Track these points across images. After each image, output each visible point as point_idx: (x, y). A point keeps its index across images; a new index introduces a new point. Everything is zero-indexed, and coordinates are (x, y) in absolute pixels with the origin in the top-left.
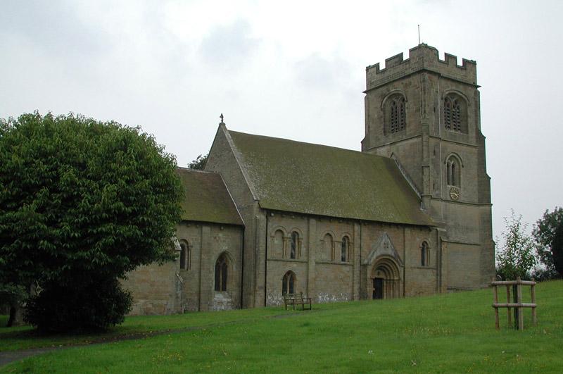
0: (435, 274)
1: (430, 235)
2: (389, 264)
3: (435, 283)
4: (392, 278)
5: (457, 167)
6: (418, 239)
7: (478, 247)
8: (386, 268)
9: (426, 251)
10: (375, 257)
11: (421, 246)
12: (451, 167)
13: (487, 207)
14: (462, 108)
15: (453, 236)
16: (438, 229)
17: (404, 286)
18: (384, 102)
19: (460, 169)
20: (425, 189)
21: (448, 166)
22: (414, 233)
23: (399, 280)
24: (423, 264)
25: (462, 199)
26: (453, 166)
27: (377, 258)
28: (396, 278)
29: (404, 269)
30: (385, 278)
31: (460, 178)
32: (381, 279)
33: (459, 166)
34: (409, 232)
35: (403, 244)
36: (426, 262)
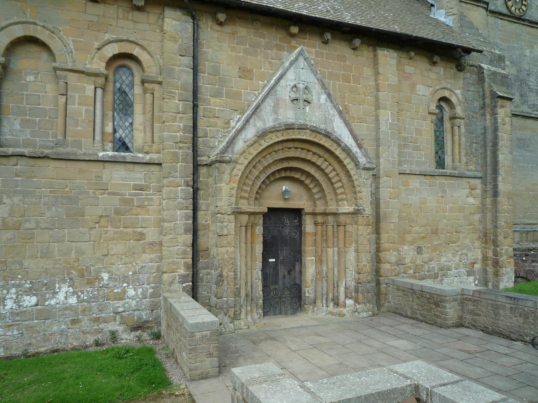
0: (478, 191)
2: (314, 159)
3: (477, 217)
4: (332, 208)
6: (421, 89)
8: (308, 175)
9: (447, 125)
10: (250, 133)
11: (433, 108)
17: (377, 231)
22: (409, 69)
23: (356, 213)
24: (440, 163)
27: (262, 135)
28: (346, 208)
29: (376, 177)
30: (308, 209)
32: (298, 213)
34: (394, 62)
35: (370, 99)
36: (448, 160)
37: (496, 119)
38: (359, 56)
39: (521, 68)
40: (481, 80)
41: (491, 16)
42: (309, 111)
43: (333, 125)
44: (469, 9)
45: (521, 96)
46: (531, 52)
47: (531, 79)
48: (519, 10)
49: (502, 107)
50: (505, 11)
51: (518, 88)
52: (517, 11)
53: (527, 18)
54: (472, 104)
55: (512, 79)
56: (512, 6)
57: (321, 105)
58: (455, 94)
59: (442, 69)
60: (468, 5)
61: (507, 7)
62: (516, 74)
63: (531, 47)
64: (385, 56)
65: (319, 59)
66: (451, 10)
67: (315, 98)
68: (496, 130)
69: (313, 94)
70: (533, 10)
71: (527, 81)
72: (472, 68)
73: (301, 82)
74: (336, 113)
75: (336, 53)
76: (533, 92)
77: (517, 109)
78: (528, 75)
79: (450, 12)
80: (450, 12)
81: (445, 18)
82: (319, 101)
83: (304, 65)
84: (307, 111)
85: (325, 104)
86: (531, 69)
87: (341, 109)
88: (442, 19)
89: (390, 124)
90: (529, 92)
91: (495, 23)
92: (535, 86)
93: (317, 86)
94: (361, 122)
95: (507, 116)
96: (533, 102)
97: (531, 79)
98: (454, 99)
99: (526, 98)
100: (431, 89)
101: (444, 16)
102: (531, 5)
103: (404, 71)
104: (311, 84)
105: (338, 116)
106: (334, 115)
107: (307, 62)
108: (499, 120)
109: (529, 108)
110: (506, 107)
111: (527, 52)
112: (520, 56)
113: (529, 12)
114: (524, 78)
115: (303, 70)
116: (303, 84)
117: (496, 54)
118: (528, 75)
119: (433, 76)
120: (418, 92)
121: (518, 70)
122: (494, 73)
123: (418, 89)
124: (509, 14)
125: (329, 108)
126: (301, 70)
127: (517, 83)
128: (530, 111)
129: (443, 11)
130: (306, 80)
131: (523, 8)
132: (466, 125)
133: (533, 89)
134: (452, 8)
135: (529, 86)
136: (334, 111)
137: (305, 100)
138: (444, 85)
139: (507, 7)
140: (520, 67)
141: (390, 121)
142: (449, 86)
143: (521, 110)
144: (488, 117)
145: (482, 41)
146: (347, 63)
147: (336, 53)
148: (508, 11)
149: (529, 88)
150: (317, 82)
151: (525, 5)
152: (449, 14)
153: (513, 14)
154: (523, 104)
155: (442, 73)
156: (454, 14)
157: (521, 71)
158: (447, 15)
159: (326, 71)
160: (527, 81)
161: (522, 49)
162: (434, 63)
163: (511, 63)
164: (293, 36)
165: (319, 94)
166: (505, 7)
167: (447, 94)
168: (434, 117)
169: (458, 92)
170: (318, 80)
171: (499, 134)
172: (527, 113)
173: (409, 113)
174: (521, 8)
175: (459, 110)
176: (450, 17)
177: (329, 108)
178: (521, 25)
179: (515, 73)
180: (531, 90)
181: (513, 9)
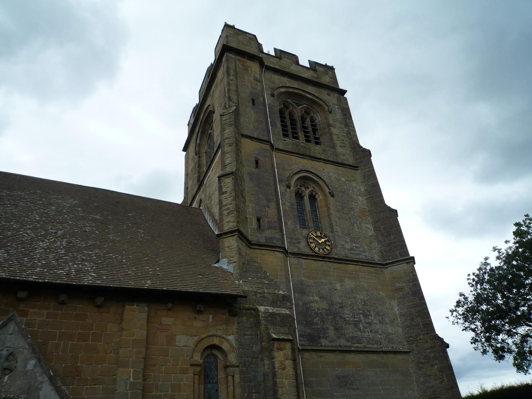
1: (235, 328)
5: (320, 197)
7: (405, 357)
11: (198, 358)
12: (306, 200)
13: (404, 267)
14: (319, 118)
15: (331, 332)
16: (262, 309)
18: (198, 142)
19: (326, 201)
20: (226, 220)
21: (299, 196)
25: (340, 252)
26: (313, 198)
31: (329, 216)
33: (325, 195)
34: (144, 315)
37: (273, 364)
38: (103, 313)
39: (333, 301)
40: (258, 323)
41: (294, 257)
42: (7, 381)
43: (38, 394)
44: (263, 254)
45: (336, 329)
46: (341, 286)
47: (346, 311)
48: (323, 249)
49: (280, 349)
50: (308, 251)
51: (332, 322)
52: (321, 250)
53: (333, 256)
54: (250, 348)
55: (323, 314)
56: (315, 247)
57: (28, 371)
58: (227, 341)
59: (211, 316)
60: (262, 251)
61: (311, 248)
62: (327, 307)
63: (342, 281)
64: (133, 311)
65: (51, 320)
66: (232, 259)
67: (20, 364)
68: (274, 375)
69: (19, 360)
70: (338, 249)
71: (341, 313)
72: (249, 311)
73: (5, 348)
74: (46, 379)
75: (75, 313)
76: (350, 324)
77: (334, 344)
78: (342, 307)
79: (232, 260)
80: (232, 260)
81: (227, 265)
82: (25, 367)
83: (14, 330)
84: (5, 381)
85: (33, 370)
86: (344, 302)
87: (52, 374)
88: (225, 267)
89: (131, 383)
90: (345, 325)
91: (299, 263)
92: (351, 317)
93: (26, 351)
94: (96, 384)
95: (287, 359)
96: (351, 335)
97: (346, 311)
98: (225, 346)
99: (342, 331)
100: (196, 338)
101: (226, 264)
102: (336, 245)
103: (161, 322)
104: (18, 350)
105: (48, 382)
106: (42, 383)
107: (18, 327)
108: (277, 365)
109: (348, 341)
110: (285, 349)
111: (338, 286)
112: (329, 290)
113: (334, 251)
114: (337, 311)
115: (12, 335)
116: (7, 350)
117: (278, 295)
118: (342, 307)
119: (198, 324)
120: (177, 344)
121: (329, 304)
122: (273, 315)
123: (177, 340)
124: (314, 254)
125: (38, 374)
126: (9, 336)
127: (330, 317)
128: (349, 344)
129: (225, 260)
130: (12, 346)
131: (328, 248)
132: (241, 373)
133: (349, 321)
134: (233, 257)
135: (344, 318)
136: (43, 378)
137: (5, 369)
138: (212, 331)
139: (311, 248)
140: (331, 301)
141: (131, 380)
142: (219, 333)
143: (338, 344)
144: (266, 362)
145: (267, 283)
146: (87, 321)
147: (75, 313)
148: (312, 251)
149: (344, 321)
150: (27, 346)
151: (329, 246)
152: (231, 262)
153: (317, 253)
154: (339, 337)
155: (211, 320)
156: (235, 262)
157: (333, 304)
158: (229, 263)
159: (57, 332)
160: (341, 313)
161: (330, 284)
162: (199, 312)
163: (320, 298)
164: (22, 300)
165: (27, 360)
166: (309, 248)
167: (216, 341)
168: (198, 369)
169: (231, 338)
170: (28, 344)
171: (278, 380)
172: (346, 346)
173: (163, 368)
174: (325, 248)
175: (232, 358)
176: (232, 265)
177: (38, 374)
178: (328, 262)
179: (327, 307)
180: (347, 322)
181: (317, 249)
